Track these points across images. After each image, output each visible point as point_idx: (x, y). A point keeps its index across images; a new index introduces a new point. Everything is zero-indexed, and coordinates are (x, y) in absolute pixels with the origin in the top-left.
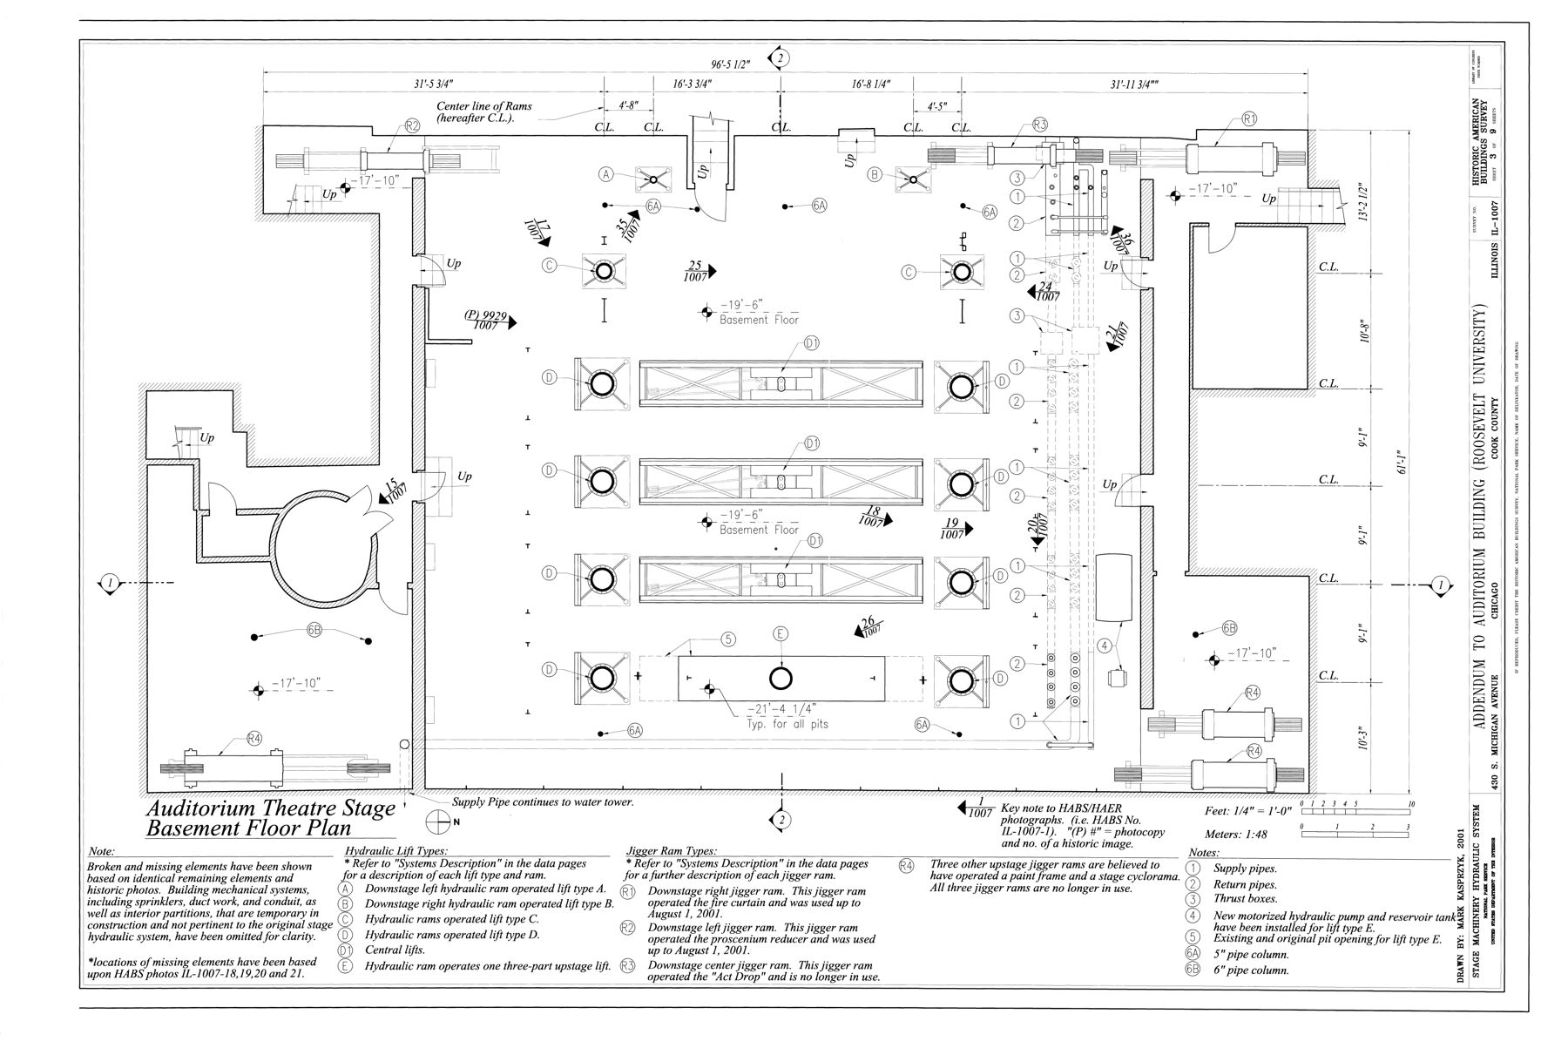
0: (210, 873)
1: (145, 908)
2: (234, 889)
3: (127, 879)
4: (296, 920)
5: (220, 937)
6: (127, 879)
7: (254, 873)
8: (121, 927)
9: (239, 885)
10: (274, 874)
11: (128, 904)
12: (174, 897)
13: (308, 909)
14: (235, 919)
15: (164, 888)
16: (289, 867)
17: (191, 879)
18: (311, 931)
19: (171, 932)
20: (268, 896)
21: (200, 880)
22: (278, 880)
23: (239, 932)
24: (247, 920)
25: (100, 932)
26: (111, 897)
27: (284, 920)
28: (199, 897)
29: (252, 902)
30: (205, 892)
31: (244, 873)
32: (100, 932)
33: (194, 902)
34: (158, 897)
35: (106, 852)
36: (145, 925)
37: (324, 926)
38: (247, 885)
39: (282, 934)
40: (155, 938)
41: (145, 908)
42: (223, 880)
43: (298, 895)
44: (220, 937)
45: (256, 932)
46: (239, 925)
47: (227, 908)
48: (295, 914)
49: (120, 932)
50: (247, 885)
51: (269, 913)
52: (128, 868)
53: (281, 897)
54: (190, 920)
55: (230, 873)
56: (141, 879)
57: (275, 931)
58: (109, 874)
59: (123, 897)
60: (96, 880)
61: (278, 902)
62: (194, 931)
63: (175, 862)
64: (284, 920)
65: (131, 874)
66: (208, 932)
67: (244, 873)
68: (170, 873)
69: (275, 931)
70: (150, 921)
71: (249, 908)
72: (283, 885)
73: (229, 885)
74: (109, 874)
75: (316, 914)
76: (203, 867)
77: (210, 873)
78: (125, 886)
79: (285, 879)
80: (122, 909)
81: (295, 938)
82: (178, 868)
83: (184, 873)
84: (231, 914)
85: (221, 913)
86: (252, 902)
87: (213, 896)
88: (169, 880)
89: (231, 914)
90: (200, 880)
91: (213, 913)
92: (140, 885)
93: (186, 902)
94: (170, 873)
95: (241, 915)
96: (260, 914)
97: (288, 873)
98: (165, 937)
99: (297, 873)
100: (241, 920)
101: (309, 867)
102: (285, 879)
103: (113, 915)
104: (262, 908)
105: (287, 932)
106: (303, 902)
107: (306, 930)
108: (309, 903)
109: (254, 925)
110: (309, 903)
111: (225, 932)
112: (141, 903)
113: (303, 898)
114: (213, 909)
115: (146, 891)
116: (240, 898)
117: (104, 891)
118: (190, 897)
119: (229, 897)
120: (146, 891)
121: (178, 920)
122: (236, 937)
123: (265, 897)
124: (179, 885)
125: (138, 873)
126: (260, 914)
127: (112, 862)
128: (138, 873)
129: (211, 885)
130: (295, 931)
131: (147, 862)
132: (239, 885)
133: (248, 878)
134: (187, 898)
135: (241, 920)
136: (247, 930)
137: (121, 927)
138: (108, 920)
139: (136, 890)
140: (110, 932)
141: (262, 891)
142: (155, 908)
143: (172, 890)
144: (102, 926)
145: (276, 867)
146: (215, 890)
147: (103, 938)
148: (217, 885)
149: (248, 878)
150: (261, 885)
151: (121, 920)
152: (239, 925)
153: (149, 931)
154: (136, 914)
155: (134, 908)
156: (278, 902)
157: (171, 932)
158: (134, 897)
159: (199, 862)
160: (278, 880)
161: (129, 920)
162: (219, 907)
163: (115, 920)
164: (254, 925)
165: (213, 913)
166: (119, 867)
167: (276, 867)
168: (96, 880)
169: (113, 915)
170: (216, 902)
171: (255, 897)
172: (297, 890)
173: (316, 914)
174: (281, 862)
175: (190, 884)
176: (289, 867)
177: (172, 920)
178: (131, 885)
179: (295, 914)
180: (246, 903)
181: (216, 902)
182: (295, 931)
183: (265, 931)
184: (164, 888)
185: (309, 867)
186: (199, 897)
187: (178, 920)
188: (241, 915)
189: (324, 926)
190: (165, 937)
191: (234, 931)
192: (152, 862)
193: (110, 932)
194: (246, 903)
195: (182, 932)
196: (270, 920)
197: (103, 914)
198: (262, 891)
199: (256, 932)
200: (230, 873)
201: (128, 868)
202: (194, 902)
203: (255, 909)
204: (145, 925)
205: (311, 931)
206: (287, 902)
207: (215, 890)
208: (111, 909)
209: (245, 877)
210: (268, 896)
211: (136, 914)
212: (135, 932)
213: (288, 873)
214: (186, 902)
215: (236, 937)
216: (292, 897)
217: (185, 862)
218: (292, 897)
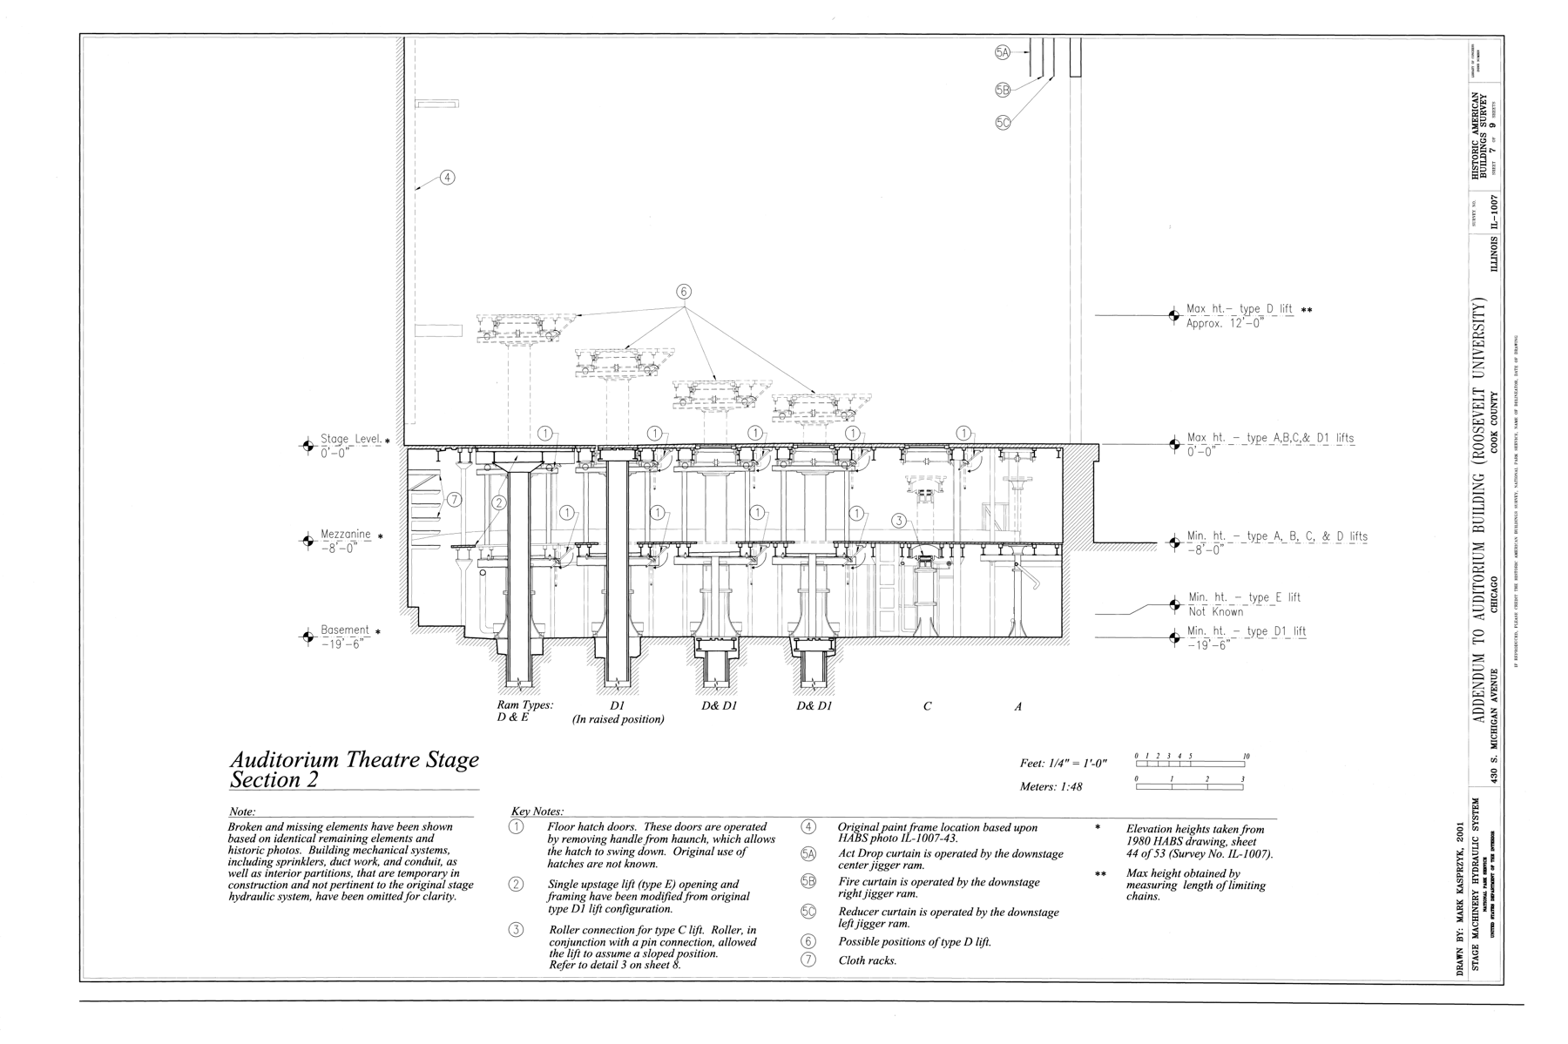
0: (351, 834)
1: (285, 868)
2: (375, 850)
3: (268, 839)
4: (437, 880)
5: (361, 897)
6: (268, 839)
7: (394, 833)
8: (262, 886)
9: (379, 846)
10: (414, 834)
11: (269, 864)
12: (315, 857)
13: (449, 869)
14: (376, 879)
15: (305, 848)
16: (430, 827)
17: (333, 839)
18: (452, 891)
19: (312, 892)
20: (409, 856)
21: (341, 840)
22: (419, 840)
23: (380, 892)
24: (387, 880)
25: (240, 892)
26: (252, 857)
27: (424, 880)
28: (340, 857)
29: (393, 862)
30: (346, 852)
31: (384, 833)
32: (240, 892)
33: (335, 862)
34: (298, 857)
35: (247, 813)
36: (285, 885)
37: (465, 886)
38: (388, 845)
39: (422, 893)
40: (296, 897)
41: (285, 868)
42: (364, 840)
43: (439, 856)
44: (361, 897)
45: (397, 892)
46: (380, 886)
47: (368, 869)
48: (436, 874)
49: (261, 892)
50: (388, 845)
51: (410, 873)
52: (269, 828)
53: (422, 857)
54: (330, 880)
55: (370, 833)
56: (282, 839)
57: (416, 891)
58: (250, 834)
59: (264, 857)
60: (237, 840)
61: (419, 862)
62: (335, 891)
63: (316, 822)
64: (424, 880)
65: (272, 834)
66: (349, 892)
67: (384, 833)
68: (310, 833)
69: (416, 891)
70: (291, 881)
71: (390, 868)
72: (424, 845)
73: (370, 845)
74: (250, 834)
75: (457, 874)
76: (344, 827)
77: (351, 834)
78: (266, 846)
79: (425, 839)
80: (263, 869)
81: (436, 898)
82: (319, 829)
83: (325, 834)
84: (372, 874)
85: (362, 873)
86: (393, 862)
87: (353, 857)
88: (310, 840)
89: (372, 874)
90: (341, 840)
91: (354, 873)
92: (281, 846)
93: (327, 862)
94: (310, 833)
95: (382, 874)
96: (401, 874)
97: (428, 834)
98: (306, 897)
99: (438, 833)
100: (382, 880)
101: (450, 827)
102: (425, 839)
103: (254, 875)
104: (403, 868)
105: (427, 891)
106: (443, 862)
107: (446, 890)
108: (450, 863)
109: (395, 885)
110: (450, 863)
111: (366, 892)
112: (281, 863)
113: (444, 858)
114: (354, 869)
115: (287, 851)
116: (381, 858)
117: (244, 851)
118: (332, 857)
119: (371, 857)
120: (287, 851)
121: (319, 880)
122: (377, 897)
123: (405, 857)
124: (320, 845)
125: (279, 834)
126: (401, 874)
127: (253, 822)
128: (279, 834)
129: (352, 846)
130: (436, 892)
131: (288, 822)
132: (379, 846)
133: (389, 839)
134: (328, 858)
135: (382, 880)
136: (387, 890)
137: (262, 886)
138: (249, 880)
139: (277, 850)
140: (251, 892)
141: (403, 851)
142: (296, 868)
143: (313, 850)
144: (242, 885)
145: (416, 827)
146: (356, 850)
147: (244, 897)
148: (358, 845)
149: (389, 839)
150: (400, 845)
151: (262, 880)
152: (380, 886)
153: (289, 891)
154: (277, 874)
155: (275, 868)
156: (419, 862)
157: (312, 892)
158: (275, 857)
159: (339, 822)
160: (419, 840)
161: (270, 880)
162: (360, 867)
163: (256, 880)
164: (395, 885)
165: (354, 873)
166: (259, 827)
167: (416, 827)
168: (237, 840)
169: (254, 875)
170: (357, 863)
171: (396, 857)
172: (438, 850)
173: (457, 874)
174: (422, 823)
175: (331, 845)
176: (430, 827)
177: (313, 880)
178: (272, 845)
179: (436, 874)
180: (387, 863)
181: (357, 863)
182: (436, 892)
183: (406, 891)
184: (305, 848)
185: (450, 827)
186: (340, 857)
187: (319, 880)
188: (382, 874)
189: (465, 886)
190: (306, 897)
191: (375, 891)
192: (293, 822)
193: (251, 892)
194: (387, 863)
195: (323, 892)
196: (411, 880)
197: (244, 874)
198: (403, 851)
199: (397, 892)
200: (370, 833)
201: (269, 828)
202: (335, 862)
203: (396, 869)
204: (285, 885)
205: (452, 891)
206: (428, 862)
207: (356, 850)
208: (252, 869)
209: (384, 838)
210: (409, 856)
211: (277, 874)
212: (276, 892)
213: (428, 834)
214: (327, 862)
215: (377, 897)
216: (432, 857)
217: (326, 822)
218: (432, 857)
